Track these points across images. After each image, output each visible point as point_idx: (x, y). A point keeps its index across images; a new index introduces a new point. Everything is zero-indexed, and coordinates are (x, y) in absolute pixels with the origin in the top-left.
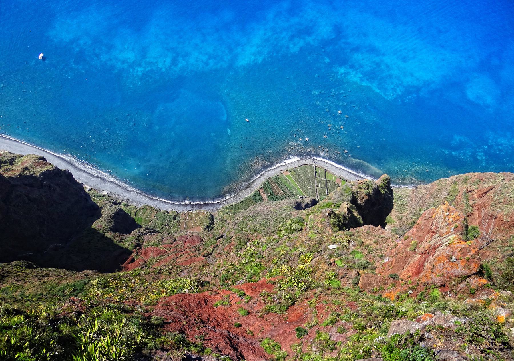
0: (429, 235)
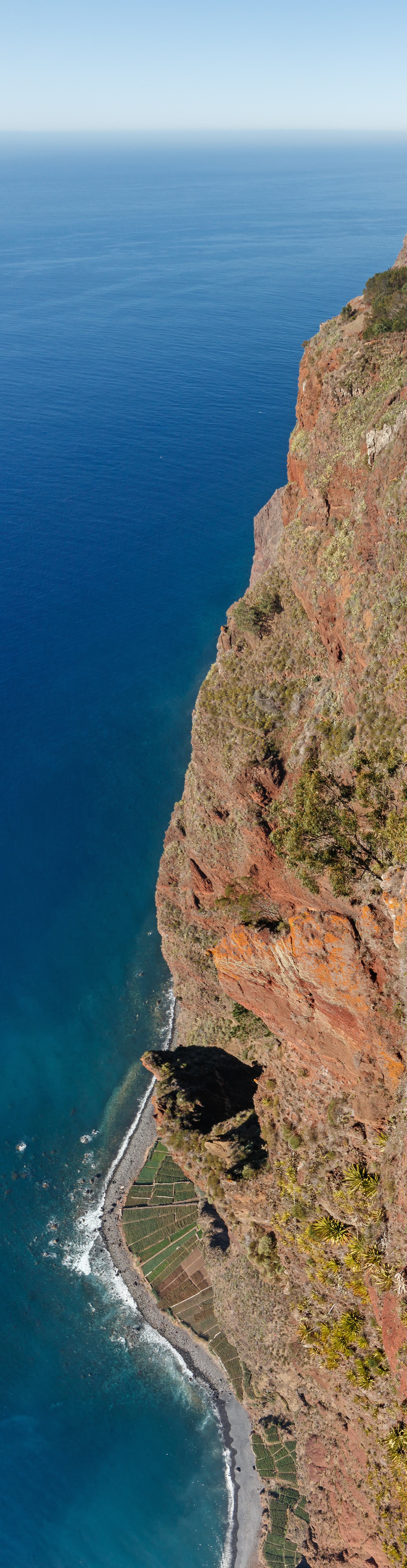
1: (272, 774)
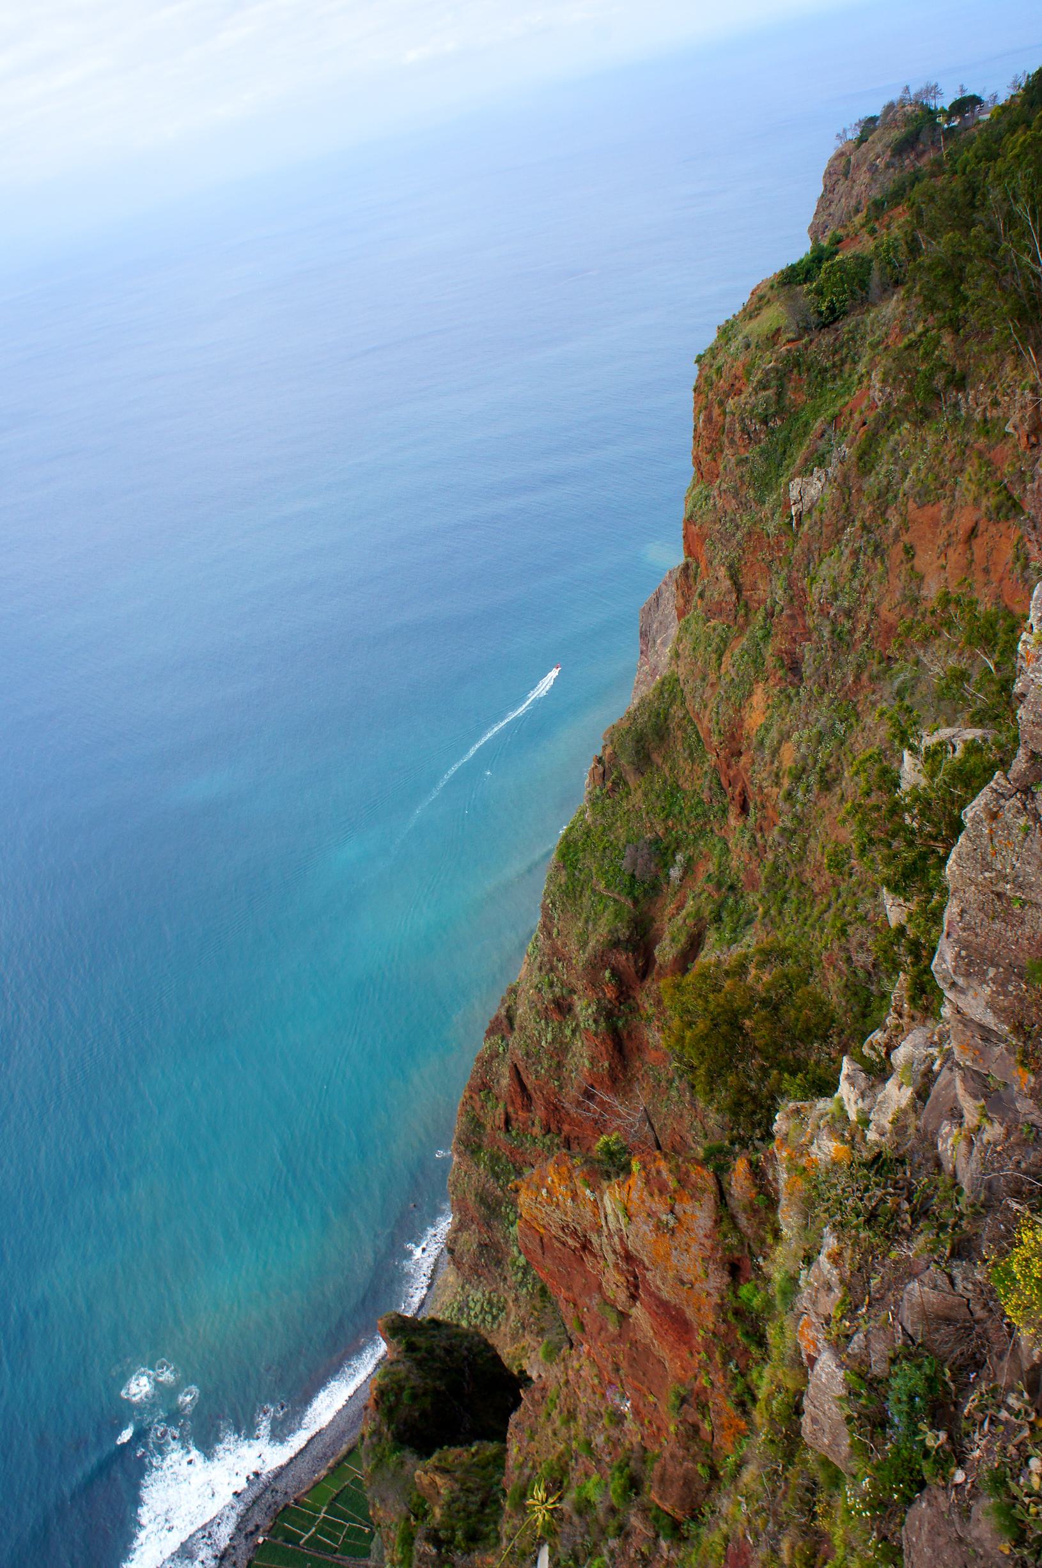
0: (589, 1261)
1: (636, 962)
